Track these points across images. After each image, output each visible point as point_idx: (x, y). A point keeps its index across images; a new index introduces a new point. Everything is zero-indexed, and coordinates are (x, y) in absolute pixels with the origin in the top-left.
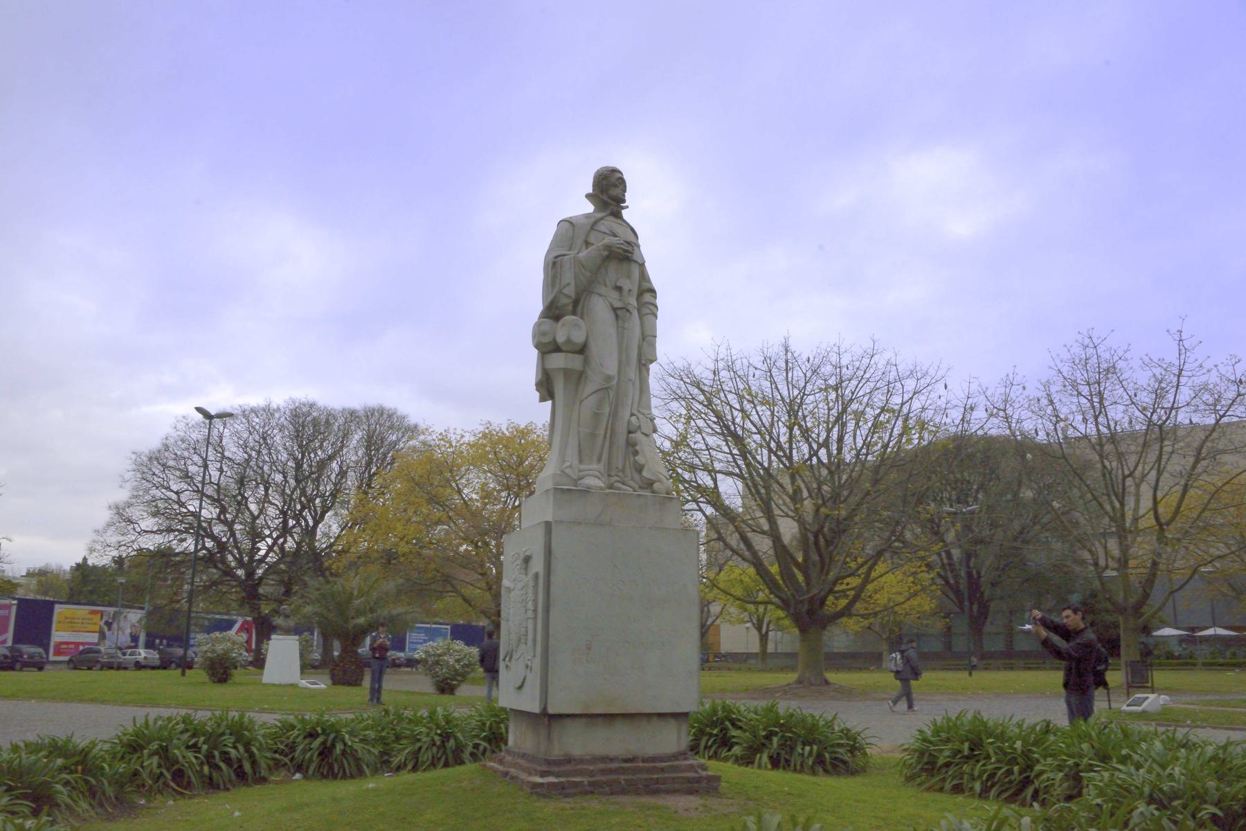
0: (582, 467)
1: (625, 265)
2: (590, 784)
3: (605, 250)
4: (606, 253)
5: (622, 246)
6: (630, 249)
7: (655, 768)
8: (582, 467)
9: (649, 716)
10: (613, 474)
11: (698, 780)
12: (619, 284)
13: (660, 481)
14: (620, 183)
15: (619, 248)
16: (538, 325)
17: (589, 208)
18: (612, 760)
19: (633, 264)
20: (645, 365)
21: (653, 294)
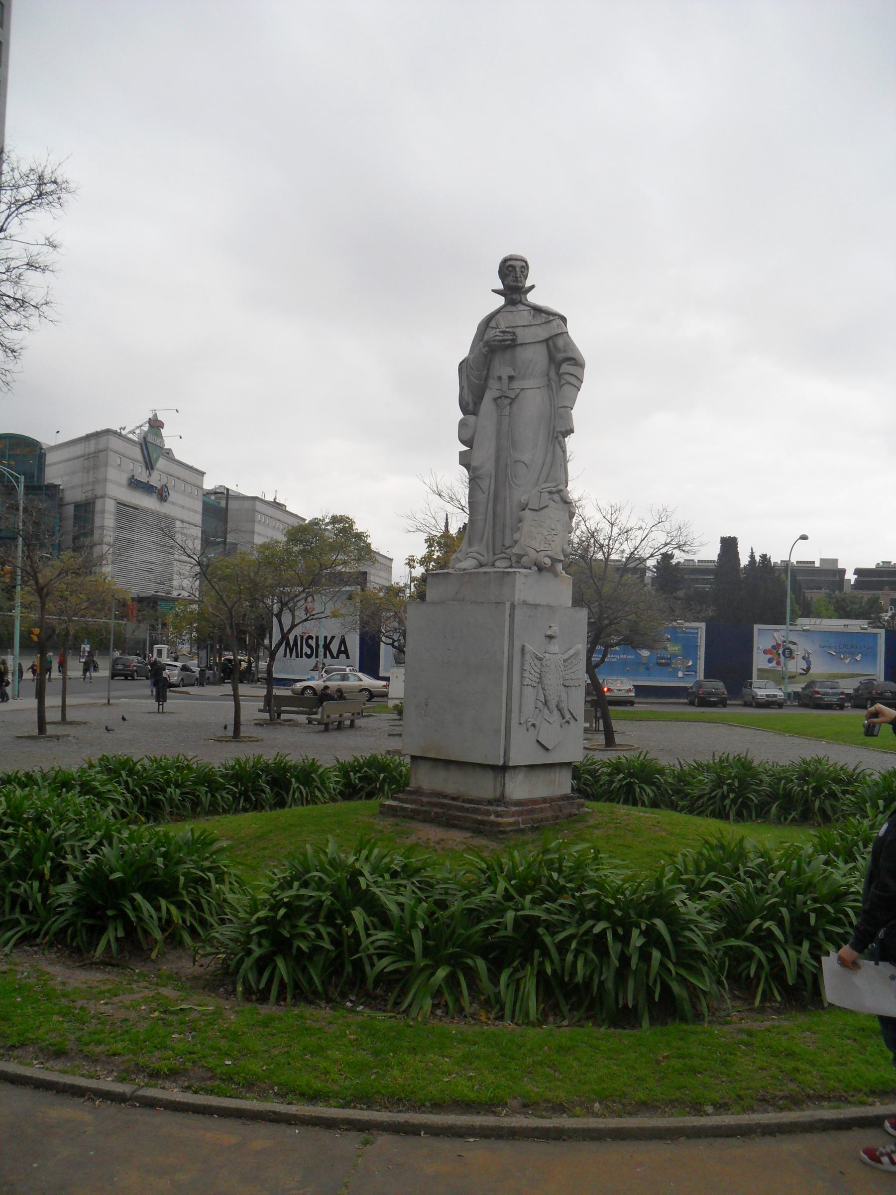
0: (469, 550)
2: (412, 810)
3: (484, 347)
4: (484, 350)
5: (498, 338)
6: (509, 337)
7: (463, 807)
8: (469, 550)
9: (474, 765)
10: (496, 553)
11: (483, 823)
12: (498, 375)
13: (526, 554)
14: (510, 271)
15: (494, 341)
16: (462, 424)
17: (500, 301)
18: (445, 796)
19: (519, 348)
20: (557, 437)
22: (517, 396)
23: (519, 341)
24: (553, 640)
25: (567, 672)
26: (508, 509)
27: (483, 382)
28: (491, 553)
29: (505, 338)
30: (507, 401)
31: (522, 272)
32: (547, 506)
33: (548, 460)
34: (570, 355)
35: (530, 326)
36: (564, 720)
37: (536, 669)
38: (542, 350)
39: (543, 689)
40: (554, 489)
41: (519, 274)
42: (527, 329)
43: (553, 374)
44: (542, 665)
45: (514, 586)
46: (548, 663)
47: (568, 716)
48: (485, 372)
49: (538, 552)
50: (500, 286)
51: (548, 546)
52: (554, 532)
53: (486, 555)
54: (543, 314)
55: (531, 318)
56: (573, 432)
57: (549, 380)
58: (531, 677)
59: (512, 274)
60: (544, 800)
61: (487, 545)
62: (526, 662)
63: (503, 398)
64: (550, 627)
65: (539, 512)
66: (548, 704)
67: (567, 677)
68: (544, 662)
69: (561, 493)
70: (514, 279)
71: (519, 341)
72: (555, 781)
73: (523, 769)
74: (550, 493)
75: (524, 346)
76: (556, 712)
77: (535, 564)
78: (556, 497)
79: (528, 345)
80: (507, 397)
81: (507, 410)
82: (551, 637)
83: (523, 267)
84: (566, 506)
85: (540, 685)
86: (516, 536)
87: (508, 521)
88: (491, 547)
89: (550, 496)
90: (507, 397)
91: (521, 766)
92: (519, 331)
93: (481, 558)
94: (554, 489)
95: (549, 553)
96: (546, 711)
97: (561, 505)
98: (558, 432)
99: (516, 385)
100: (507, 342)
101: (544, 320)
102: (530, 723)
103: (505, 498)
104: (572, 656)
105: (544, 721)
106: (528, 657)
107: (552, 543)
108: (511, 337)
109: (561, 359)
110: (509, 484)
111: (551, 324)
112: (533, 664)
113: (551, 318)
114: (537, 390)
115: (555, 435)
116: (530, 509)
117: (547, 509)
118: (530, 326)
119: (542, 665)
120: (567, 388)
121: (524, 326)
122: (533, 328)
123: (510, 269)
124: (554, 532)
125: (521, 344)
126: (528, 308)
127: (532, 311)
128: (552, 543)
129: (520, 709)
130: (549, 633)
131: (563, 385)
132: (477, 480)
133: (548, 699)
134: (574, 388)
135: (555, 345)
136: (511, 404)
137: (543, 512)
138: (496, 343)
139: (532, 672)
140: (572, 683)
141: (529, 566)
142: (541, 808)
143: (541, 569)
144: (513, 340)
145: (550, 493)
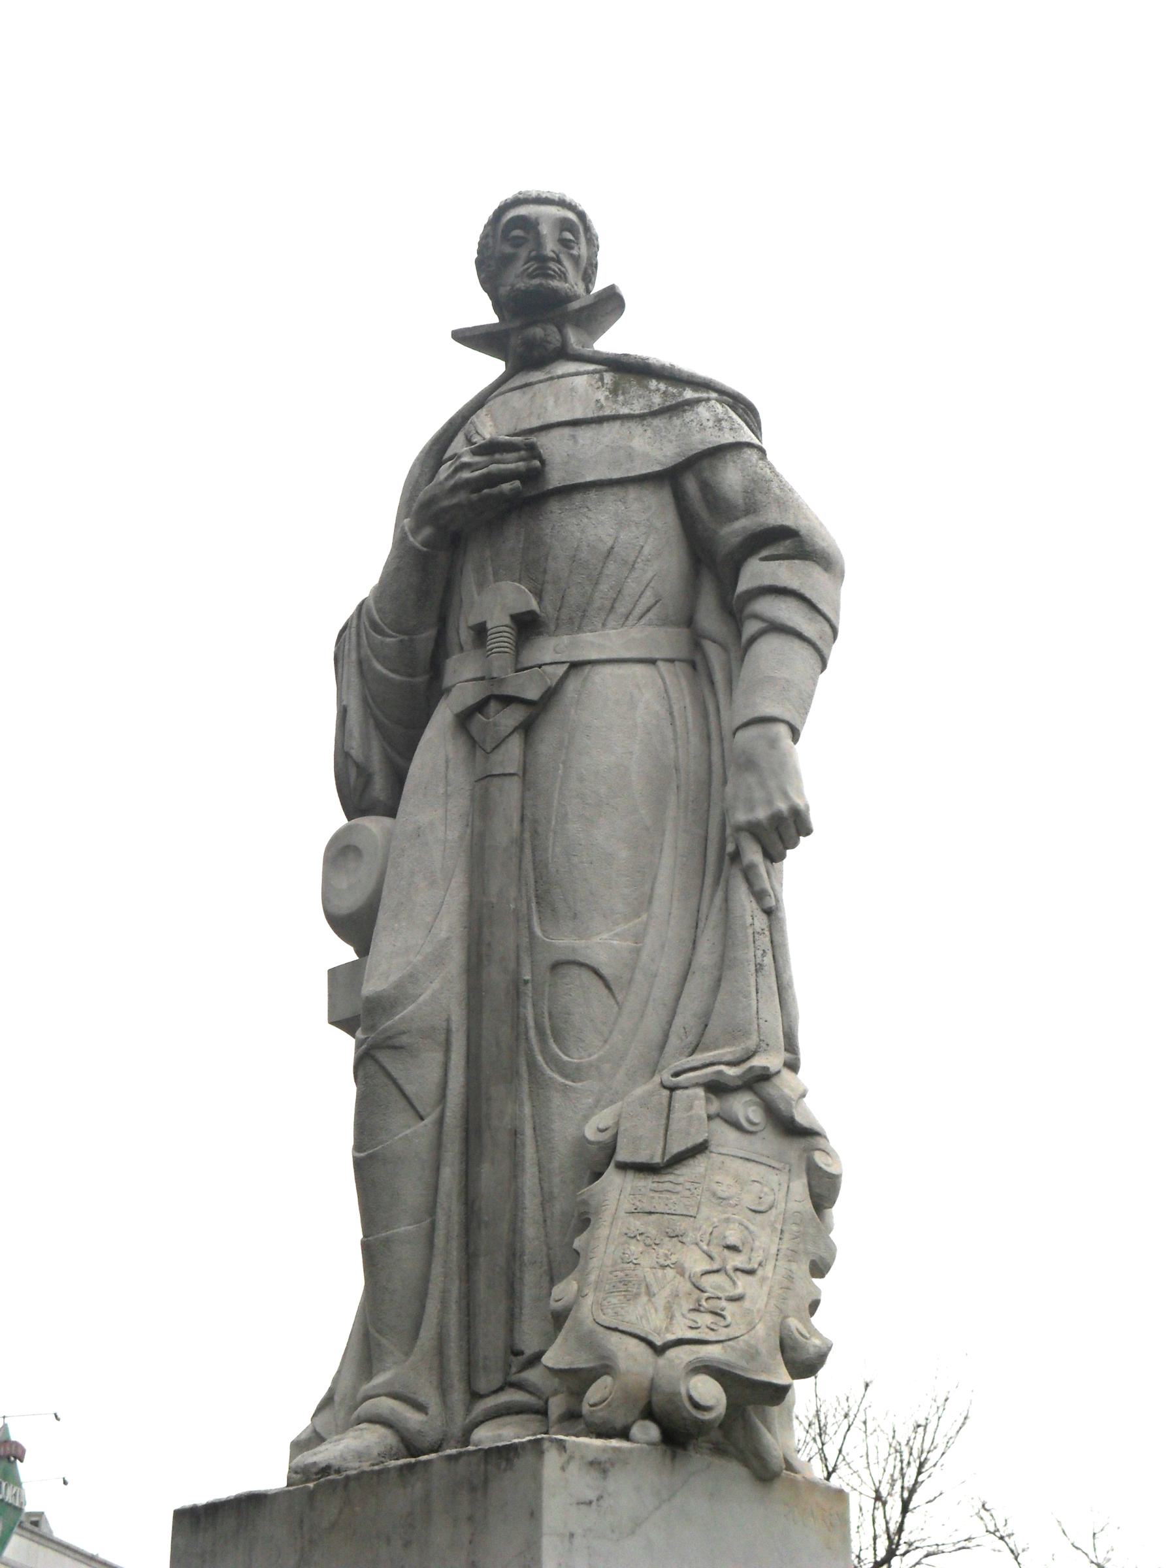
1: (513, 538)
5: (466, 475)
6: (511, 463)
10: (482, 1385)
13: (605, 1368)
14: (518, 243)
19: (555, 507)
20: (736, 856)
21: (780, 549)
22: (551, 694)
23: (556, 478)
26: (530, 1179)
27: (421, 679)
28: (458, 1396)
30: (510, 718)
31: (565, 243)
32: (701, 1149)
33: (705, 956)
34: (773, 517)
35: (599, 420)
40: (731, 1071)
41: (550, 247)
42: (585, 435)
43: (710, 619)
45: (534, 1514)
48: (427, 635)
49: (659, 1350)
50: (483, 313)
51: (708, 1319)
52: (737, 1260)
53: (429, 1396)
54: (653, 384)
55: (601, 395)
56: (808, 831)
57: (696, 641)
59: (523, 253)
61: (440, 1351)
63: (493, 706)
69: (769, 1089)
70: (533, 266)
71: (556, 478)
74: (717, 1088)
75: (578, 498)
77: (649, 1413)
78: (744, 1107)
79: (593, 495)
80: (507, 701)
81: (512, 752)
83: (564, 225)
84: (793, 1149)
86: (565, 1290)
87: (531, 1231)
88: (455, 1367)
89: (715, 1106)
90: (507, 701)
92: (553, 446)
93: (412, 1418)
94: (731, 1071)
95: (713, 1352)
97: (768, 1142)
98: (739, 829)
100: (506, 487)
101: (657, 401)
103: (515, 1133)
107: (730, 1309)
109: (735, 540)
110: (532, 1065)
111: (689, 416)
113: (689, 394)
114: (639, 669)
115: (730, 848)
116: (624, 1167)
118: (599, 420)
120: (769, 649)
121: (575, 423)
122: (610, 433)
123: (517, 232)
124: (737, 1260)
125: (568, 491)
126: (591, 367)
127: (608, 377)
128: (730, 1309)
131: (753, 640)
132: (384, 1057)
134: (797, 644)
135: (709, 491)
136: (527, 728)
138: (462, 497)
141: (619, 1422)
144: (533, 476)
145: (717, 1088)
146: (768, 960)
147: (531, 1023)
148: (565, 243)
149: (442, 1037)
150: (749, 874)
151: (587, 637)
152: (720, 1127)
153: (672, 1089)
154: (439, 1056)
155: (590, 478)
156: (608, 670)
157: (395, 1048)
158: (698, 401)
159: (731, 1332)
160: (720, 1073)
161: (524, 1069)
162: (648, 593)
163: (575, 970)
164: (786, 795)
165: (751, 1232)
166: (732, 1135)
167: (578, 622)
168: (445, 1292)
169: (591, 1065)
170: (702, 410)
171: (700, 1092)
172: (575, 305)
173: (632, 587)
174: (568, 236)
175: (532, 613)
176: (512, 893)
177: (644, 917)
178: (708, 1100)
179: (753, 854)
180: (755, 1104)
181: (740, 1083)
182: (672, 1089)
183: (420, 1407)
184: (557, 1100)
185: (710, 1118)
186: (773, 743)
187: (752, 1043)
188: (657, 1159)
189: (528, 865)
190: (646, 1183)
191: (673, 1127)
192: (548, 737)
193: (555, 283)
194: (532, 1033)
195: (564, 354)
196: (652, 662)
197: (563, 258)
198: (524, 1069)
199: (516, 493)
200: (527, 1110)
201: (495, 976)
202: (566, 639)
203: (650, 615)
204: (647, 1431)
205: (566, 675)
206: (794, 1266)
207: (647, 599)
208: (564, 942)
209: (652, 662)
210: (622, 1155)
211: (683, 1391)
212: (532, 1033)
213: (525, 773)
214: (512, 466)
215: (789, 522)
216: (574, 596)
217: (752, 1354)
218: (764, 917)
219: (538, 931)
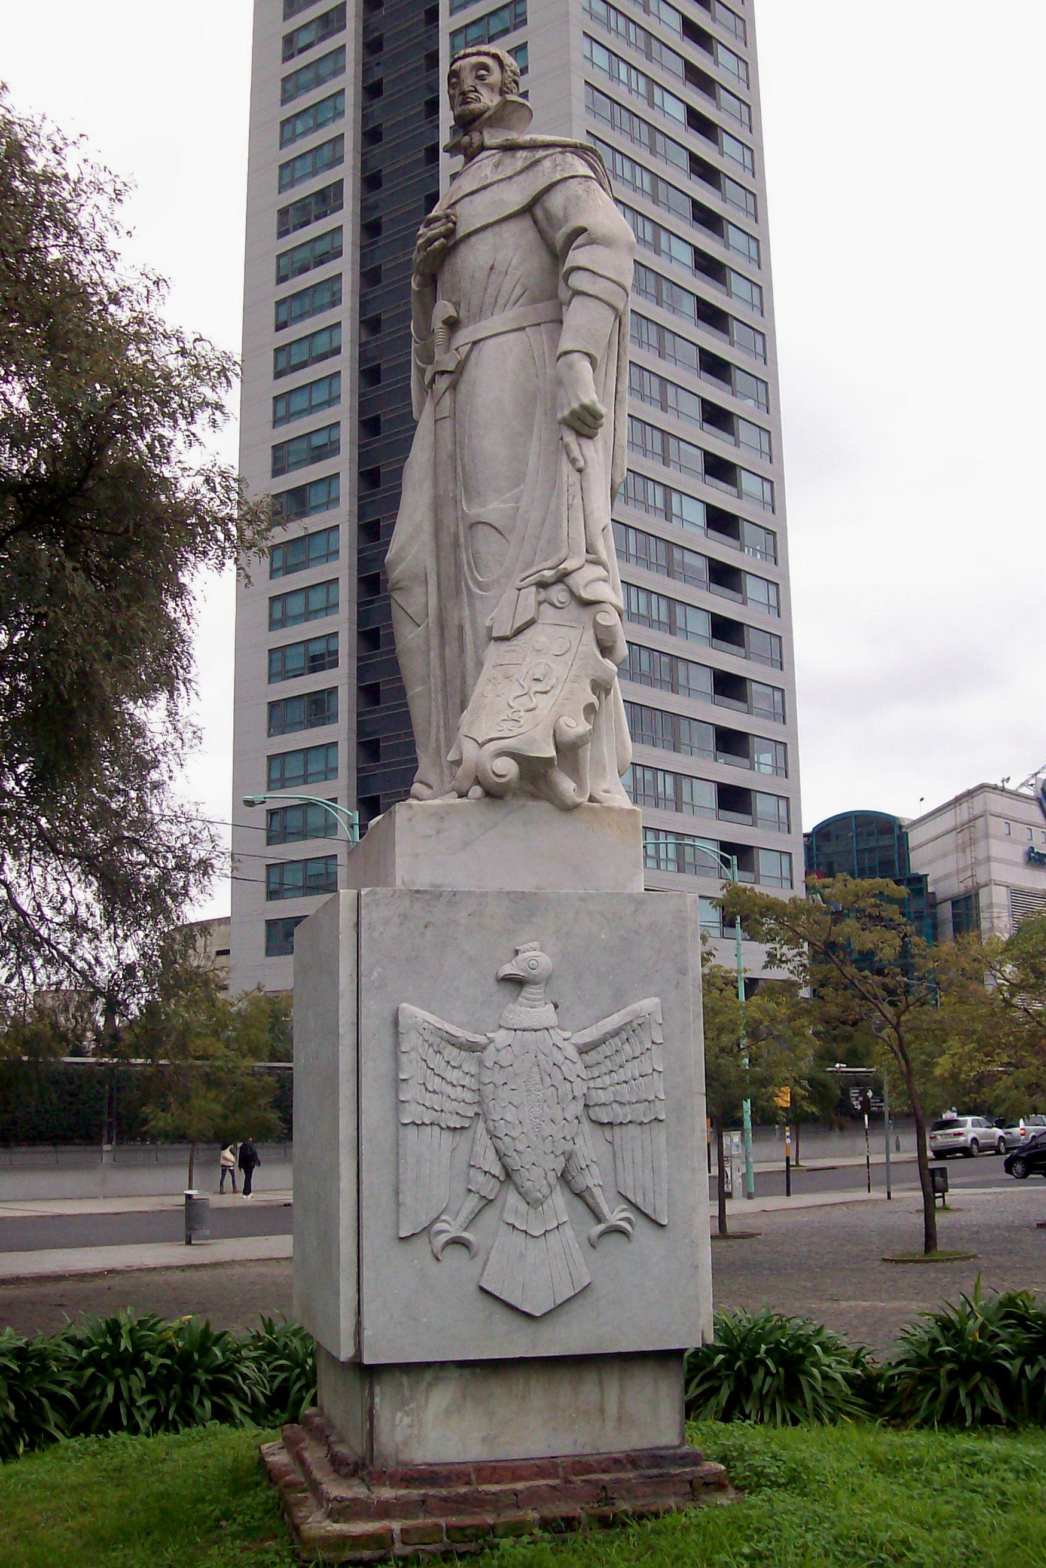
22: (462, 365)
23: (461, 232)
24: (528, 991)
25: (599, 1083)
29: (430, 234)
36: (602, 1227)
37: (453, 1075)
38: (520, 234)
39: (493, 1136)
40: (547, 573)
42: (477, 198)
44: (481, 1063)
46: (505, 1058)
47: (616, 1214)
49: (481, 745)
52: (539, 687)
58: (430, 1099)
60: (545, 1467)
62: (404, 1059)
64: (517, 952)
65: (514, 642)
66: (516, 1178)
67: (602, 1096)
68: (489, 1057)
71: (461, 232)
72: (602, 1411)
73: (455, 1373)
75: (474, 239)
76: (559, 1201)
77: (478, 782)
78: (557, 594)
82: (516, 983)
84: (586, 615)
85: (481, 1125)
89: (543, 595)
90: (443, 373)
91: (443, 1365)
94: (547, 573)
96: (512, 1199)
99: (464, 336)
100: (436, 243)
101: (520, 165)
102: (444, 1238)
103: (461, 628)
104: (616, 1033)
105: (504, 1228)
106: (410, 1041)
108: (442, 229)
111: (539, 168)
112: (436, 1061)
113: (541, 153)
114: (512, 336)
117: (532, 628)
119: (481, 1063)
124: (539, 687)
129: (397, 1194)
130: (507, 969)
133: (514, 1162)
135: (547, 214)
136: (454, 387)
137: (521, 638)
139: (436, 1083)
140: (619, 1113)
142: (515, 1494)
143: (494, 794)
144: (450, 234)
145: (542, 585)
146: (578, 501)
147: (465, 561)
148: (481, 78)
149: (423, 579)
150: (567, 448)
151: (483, 323)
152: (545, 607)
153: (520, 590)
154: (423, 589)
155: (478, 226)
156: (491, 342)
157: (398, 589)
158: (546, 157)
159: (521, 731)
160: (543, 576)
161: (464, 589)
162: (518, 287)
163: (480, 526)
164: (577, 397)
165: (551, 669)
166: (550, 610)
167: (479, 315)
168: (438, 722)
169: (493, 581)
170: (547, 163)
171: (533, 589)
172: (486, 115)
173: (507, 287)
174: (483, 72)
175: (451, 317)
176: (451, 487)
177: (522, 487)
178: (538, 593)
179: (570, 438)
180: (563, 590)
181: (553, 580)
182: (520, 590)
183: (430, 787)
184: (478, 604)
185: (540, 603)
186: (570, 367)
187: (562, 555)
188: (508, 633)
189: (459, 470)
190: (505, 646)
191: (519, 610)
192: (463, 387)
193: (472, 106)
194: (466, 567)
195: (483, 148)
196: (523, 329)
197: (479, 88)
198: (464, 589)
199: (443, 246)
200: (467, 612)
201: (446, 540)
202: (471, 328)
203: (522, 300)
204: (476, 791)
205: (471, 350)
206: (575, 685)
207: (518, 291)
208: (474, 511)
209: (523, 329)
210: (495, 634)
211: (489, 768)
212: (466, 567)
213: (453, 415)
214: (437, 231)
215: (581, 223)
216: (475, 301)
217: (532, 741)
218: (577, 474)
219: (465, 509)
